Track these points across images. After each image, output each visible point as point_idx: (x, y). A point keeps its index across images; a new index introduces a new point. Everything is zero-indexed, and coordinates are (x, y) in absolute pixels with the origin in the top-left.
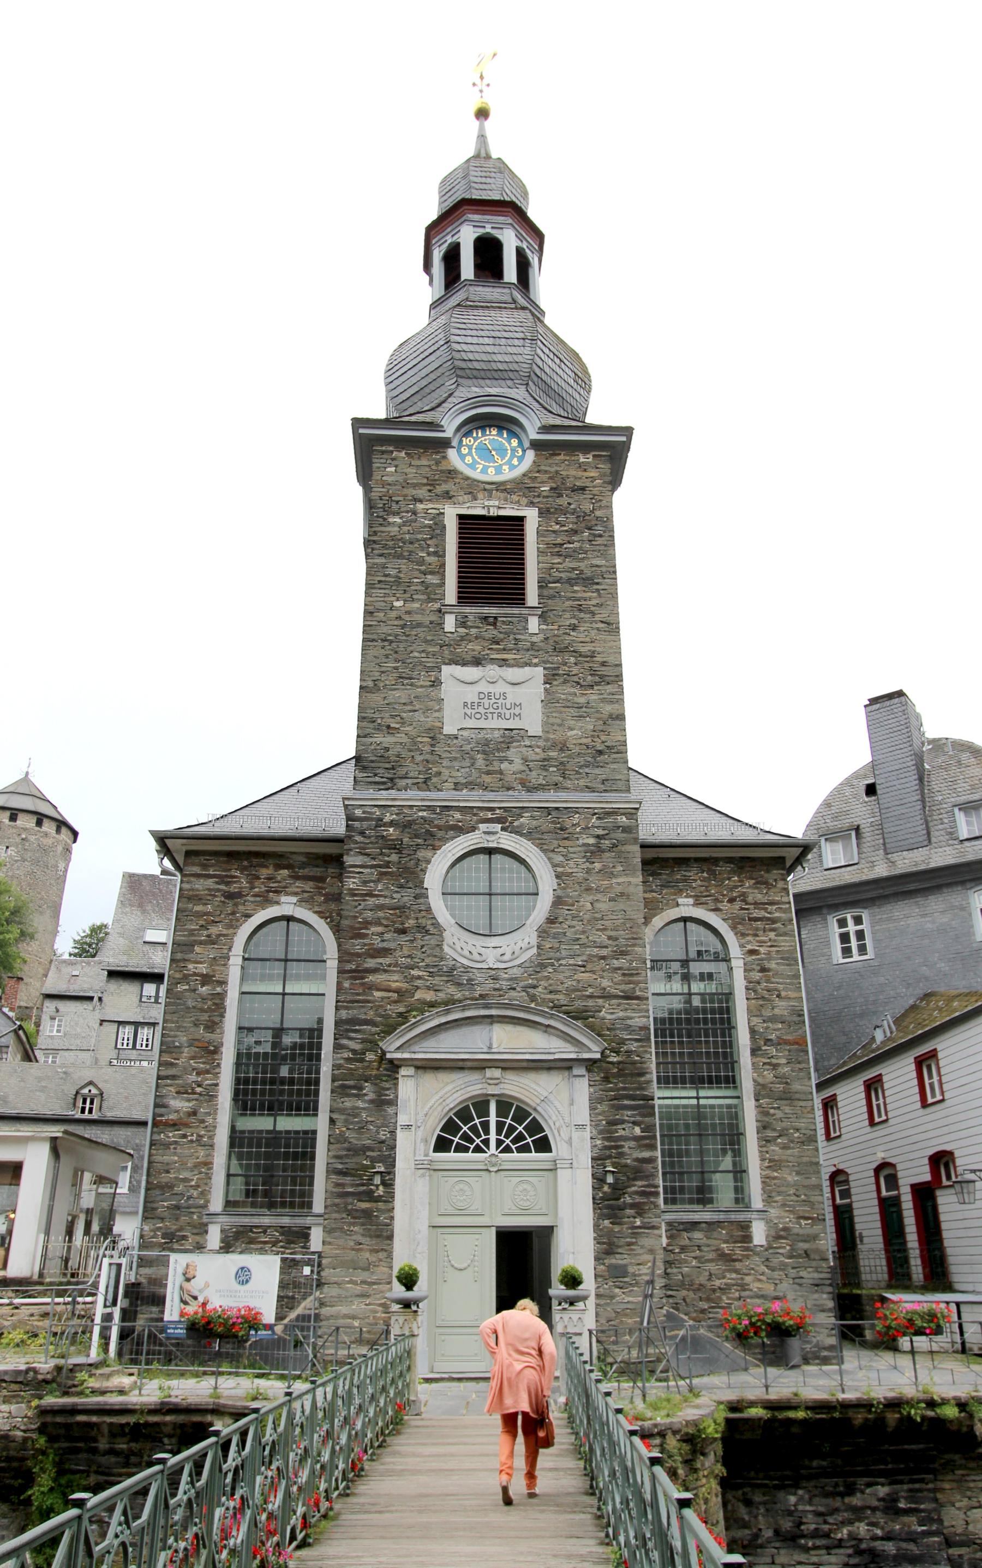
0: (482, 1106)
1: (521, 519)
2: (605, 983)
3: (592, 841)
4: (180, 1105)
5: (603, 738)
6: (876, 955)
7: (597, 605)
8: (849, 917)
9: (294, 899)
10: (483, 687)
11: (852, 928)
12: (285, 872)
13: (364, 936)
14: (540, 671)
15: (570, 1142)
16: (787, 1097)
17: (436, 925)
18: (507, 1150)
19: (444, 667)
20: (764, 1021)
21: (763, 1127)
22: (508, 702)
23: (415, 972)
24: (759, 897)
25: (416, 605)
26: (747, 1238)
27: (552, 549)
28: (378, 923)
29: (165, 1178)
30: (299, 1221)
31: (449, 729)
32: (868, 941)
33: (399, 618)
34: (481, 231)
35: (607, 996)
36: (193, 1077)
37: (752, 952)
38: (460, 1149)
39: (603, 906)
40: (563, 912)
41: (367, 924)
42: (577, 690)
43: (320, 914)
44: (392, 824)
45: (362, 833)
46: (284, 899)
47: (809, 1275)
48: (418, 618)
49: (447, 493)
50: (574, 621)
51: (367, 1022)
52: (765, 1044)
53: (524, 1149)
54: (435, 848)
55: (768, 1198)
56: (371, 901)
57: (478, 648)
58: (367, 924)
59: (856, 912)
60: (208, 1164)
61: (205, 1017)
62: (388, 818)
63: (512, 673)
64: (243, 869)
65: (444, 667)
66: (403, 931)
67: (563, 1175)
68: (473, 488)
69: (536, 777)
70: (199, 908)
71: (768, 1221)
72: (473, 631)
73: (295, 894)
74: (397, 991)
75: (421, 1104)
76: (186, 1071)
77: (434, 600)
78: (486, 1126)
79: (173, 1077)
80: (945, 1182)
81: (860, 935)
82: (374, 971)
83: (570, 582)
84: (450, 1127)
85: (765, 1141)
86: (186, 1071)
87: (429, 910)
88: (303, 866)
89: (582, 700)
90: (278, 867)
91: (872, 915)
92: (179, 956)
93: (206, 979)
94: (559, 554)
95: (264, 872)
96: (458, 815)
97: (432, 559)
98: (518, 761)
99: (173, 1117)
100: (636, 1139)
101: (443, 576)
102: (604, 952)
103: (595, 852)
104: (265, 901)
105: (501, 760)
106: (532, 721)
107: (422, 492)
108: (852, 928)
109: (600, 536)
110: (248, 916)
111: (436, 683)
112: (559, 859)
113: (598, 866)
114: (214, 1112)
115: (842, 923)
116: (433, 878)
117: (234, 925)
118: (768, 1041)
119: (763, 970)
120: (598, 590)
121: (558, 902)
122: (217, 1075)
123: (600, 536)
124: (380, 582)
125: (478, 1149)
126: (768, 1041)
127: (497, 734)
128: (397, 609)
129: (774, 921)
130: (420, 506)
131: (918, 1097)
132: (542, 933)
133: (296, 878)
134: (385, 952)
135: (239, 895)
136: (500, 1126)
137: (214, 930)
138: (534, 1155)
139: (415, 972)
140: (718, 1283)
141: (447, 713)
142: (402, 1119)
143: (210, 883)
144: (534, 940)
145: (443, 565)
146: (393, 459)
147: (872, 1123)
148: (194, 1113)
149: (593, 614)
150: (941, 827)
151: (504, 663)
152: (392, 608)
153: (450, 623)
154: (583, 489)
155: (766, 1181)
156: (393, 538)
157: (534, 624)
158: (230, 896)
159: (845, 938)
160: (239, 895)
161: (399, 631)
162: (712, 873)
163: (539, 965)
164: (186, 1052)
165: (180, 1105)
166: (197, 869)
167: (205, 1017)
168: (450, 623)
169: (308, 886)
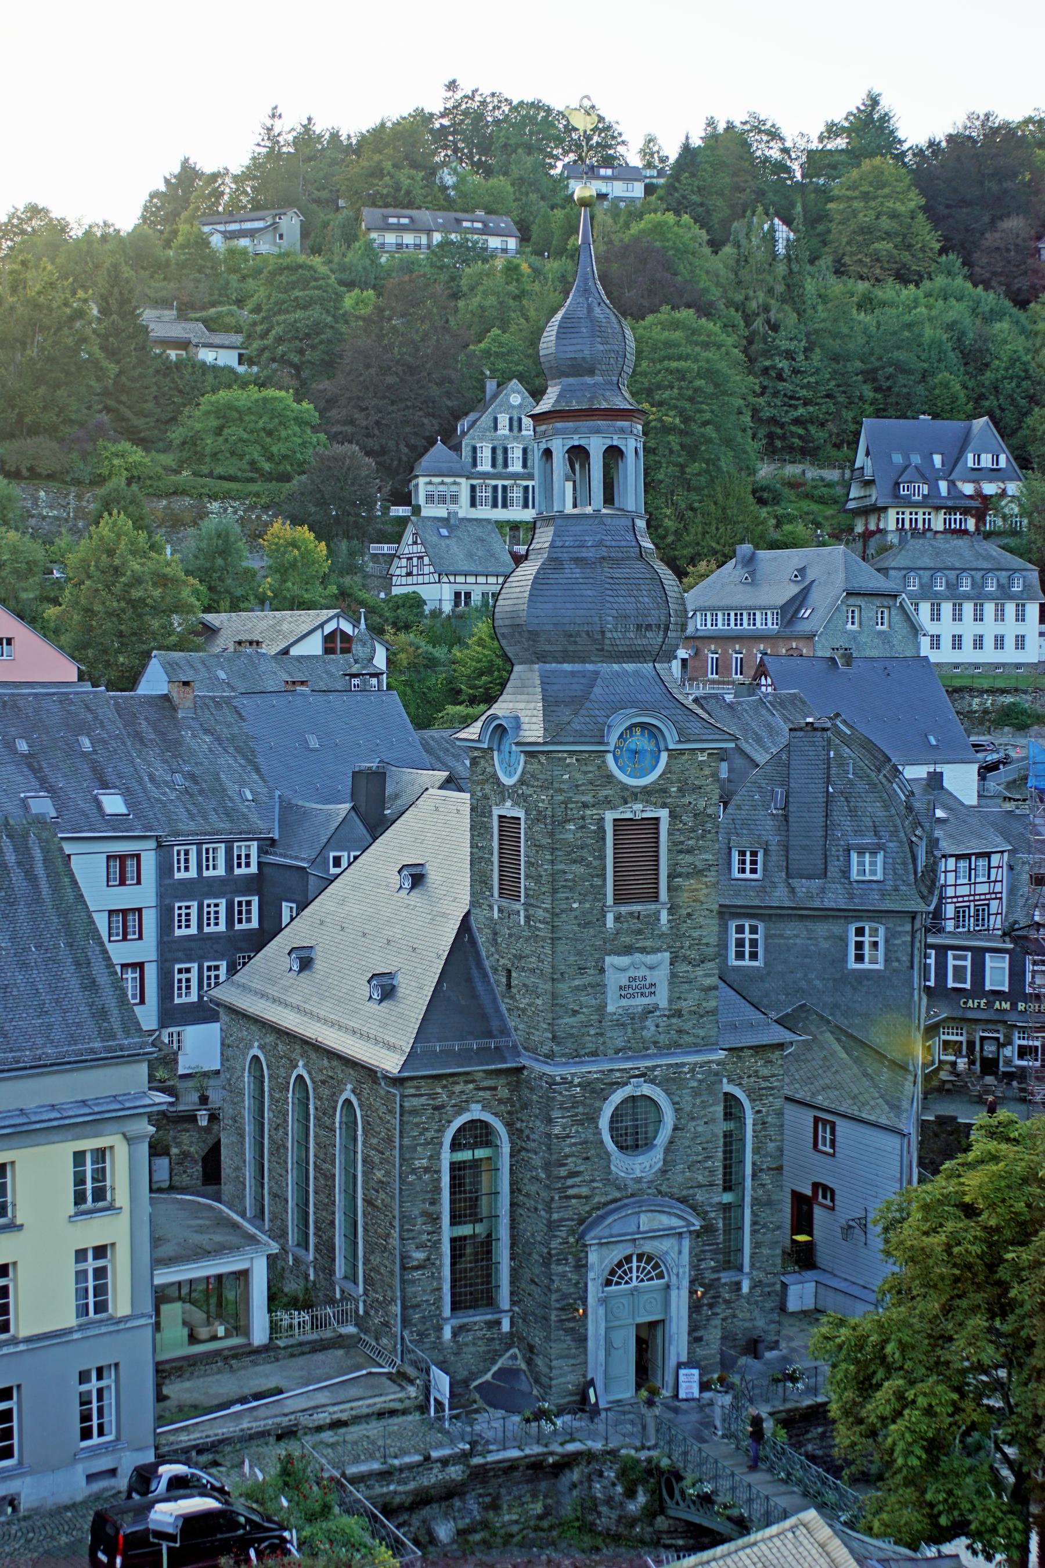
0: (628, 1259)
1: (657, 819)
2: (700, 1178)
3: (695, 1084)
4: (420, 1255)
5: (705, 1004)
6: (765, 963)
9: (479, 1106)
10: (632, 973)
11: (747, 935)
12: (471, 1086)
13: (565, 1165)
14: (667, 955)
15: (678, 1275)
16: (769, 1203)
18: (642, 1281)
19: (607, 958)
21: (754, 1223)
22: (647, 983)
23: (595, 1185)
24: (765, 1072)
25: (587, 906)
26: (739, 1289)
27: (677, 849)
28: (573, 1155)
29: (414, 1301)
30: (496, 1316)
31: (610, 1009)
32: (760, 951)
34: (609, 442)
35: (700, 1186)
36: (425, 1237)
37: (759, 1112)
38: (618, 1283)
39: (700, 1129)
40: (679, 1133)
41: (567, 1157)
42: (689, 968)
43: (495, 1114)
44: (579, 1085)
45: (560, 1093)
46: (473, 1106)
47: (769, 1305)
48: (589, 918)
49: (606, 797)
50: (689, 910)
51: (568, 1219)
53: (651, 1279)
54: (606, 1099)
55: (752, 1265)
56: (568, 1141)
57: (628, 939)
58: (567, 1157)
59: (754, 922)
60: (439, 1289)
61: (429, 1196)
62: (577, 1081)
63: (650, 959)
64: (444, 1087)
65: (607, 958)
66: (587, 1158)
67: (674, 1293)
68: (628, 795)
69: (663, 1039)
70: (416, 1120)
71: (752, 1279)
72: (625, 926)
73: (478, 1102)
74: (586, 1197)
75: (599, 1261)
76: (420, 1233)
77: (599, 900)
78: (631, 1269)
79: (413, 1238)
81: (754, 943)
82: (572, 1187)
83: (688, 876)
84: (613, 1273)
85: (754, 1232)
86: (420, 1233)
87: (602, 1142)
88: (483, 1079)
90: (467, 1082)
91: (766, 929)
93: (427, 1170)
94: (681, 852)
95: (458, 1088)
96: (618, 1074)
97: (596, 863)
98: (653, 1028)
99: (415, 1263)
100: (712, 1268)
101: (605, 880)
102: (700, 1158)
103: (696, 1093)
104: (460, 1110)
106: (662, 999)
107: (588, 798)
108: (747, 935)
109: (710, 832)
110: (450, 1122)
111: (602, 971)
113: (698, 1101)
114: (440, 1256)
115: (740, 929)
116: (604, 1123)
117: (441, 1131)
118: (761, 1170)
119: (764, 1123)
120: (705, 883)
121: (676, 1128)
122: (439, 1234)
123: (710, 832)
124: (564, 887)
125: (627, 1283)
126: (761, 1170)
127: (640, 1009)
129: (772, 1088)
130: (588, 812)
132: (667, 1151)
133: (478, 1089)
134: (577, 1174)
135: (443, 1107)
136: (638, 1267)
137: (429, 1135)
138: (656, 1282)
139: (595, 1185)
141: (609, 995)
142: (591, 1275)
143: (423, 1100)
144: (661, 1156)
145: (604, 868)
146: (568, 765)
148: (428, 1259)
151: (643, 950)
152: (572, 910)
155: (753, 1255)
157: (664, 916)
158: (436, 1108)
159: (740, 943)
160: (443, 1107)
161: (576, 928)
162: (739, 1057)
163: (664, 1172)
164: (419, 1221)
166: (412, 1091)
167: (429, 1196)
169: (487, 1094)
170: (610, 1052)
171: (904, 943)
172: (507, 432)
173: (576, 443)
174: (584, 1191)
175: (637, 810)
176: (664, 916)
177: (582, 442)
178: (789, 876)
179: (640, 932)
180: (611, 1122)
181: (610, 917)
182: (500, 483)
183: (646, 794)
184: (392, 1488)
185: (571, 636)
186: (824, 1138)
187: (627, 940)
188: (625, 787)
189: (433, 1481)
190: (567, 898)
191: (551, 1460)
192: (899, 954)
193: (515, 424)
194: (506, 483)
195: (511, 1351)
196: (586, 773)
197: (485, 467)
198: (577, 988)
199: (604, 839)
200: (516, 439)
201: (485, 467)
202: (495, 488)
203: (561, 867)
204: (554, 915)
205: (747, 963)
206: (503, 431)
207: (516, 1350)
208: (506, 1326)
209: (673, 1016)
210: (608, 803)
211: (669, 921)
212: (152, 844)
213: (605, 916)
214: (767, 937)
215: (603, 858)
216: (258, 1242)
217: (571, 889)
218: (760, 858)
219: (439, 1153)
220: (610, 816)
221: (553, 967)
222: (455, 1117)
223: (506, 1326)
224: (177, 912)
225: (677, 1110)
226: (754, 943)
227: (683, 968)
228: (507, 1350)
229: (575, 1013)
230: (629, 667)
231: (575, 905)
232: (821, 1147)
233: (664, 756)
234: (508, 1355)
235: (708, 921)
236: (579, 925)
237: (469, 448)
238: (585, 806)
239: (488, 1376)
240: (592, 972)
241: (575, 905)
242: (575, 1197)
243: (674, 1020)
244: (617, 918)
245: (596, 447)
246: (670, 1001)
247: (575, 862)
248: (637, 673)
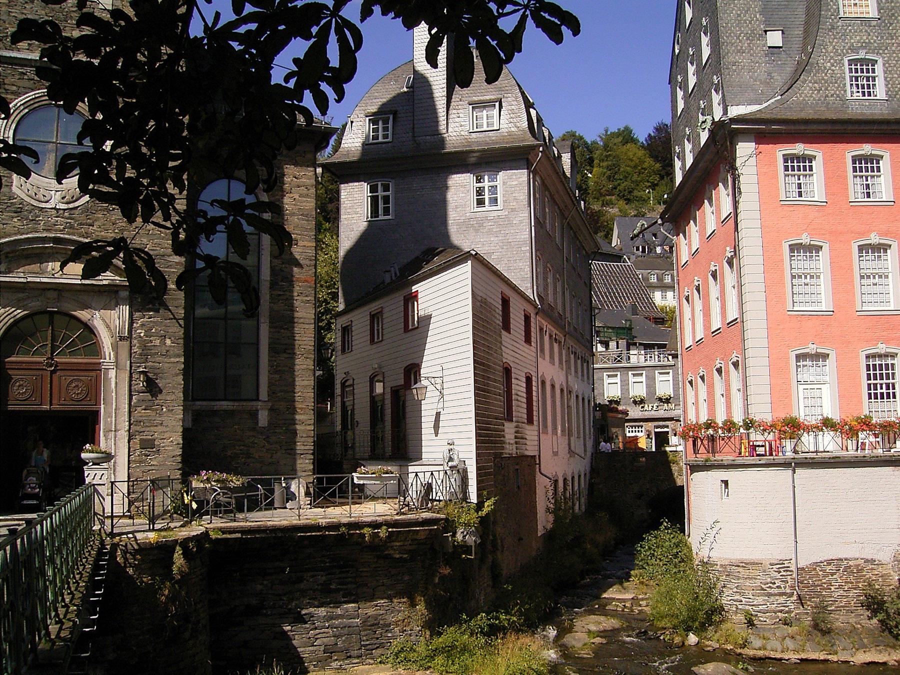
8: (379, 183)
11: (380, 193)
20: (283, 263)
52: (282, 281)
81: (386, 200)
131: (402, 325)
140: (229, 453)
147: (372, 341)
150: (457, 120)
205: (381, 218)
214: (396, 193)
226: (386, 200)
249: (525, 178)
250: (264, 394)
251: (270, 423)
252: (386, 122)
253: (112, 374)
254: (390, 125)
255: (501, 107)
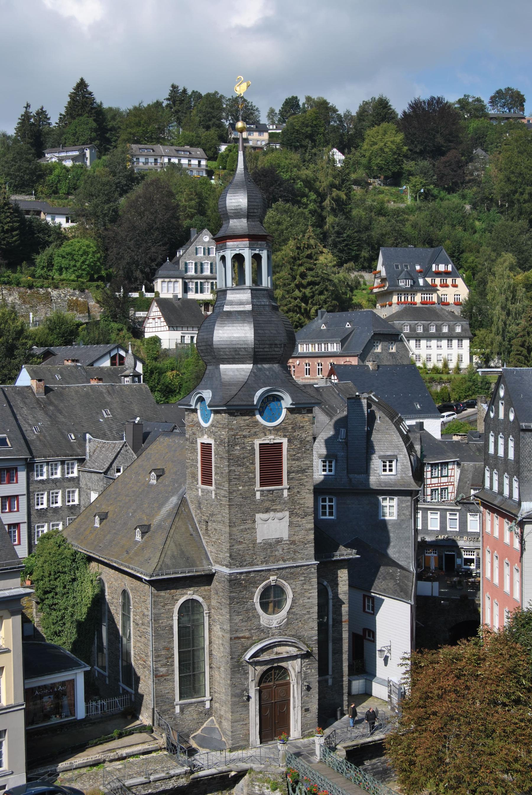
1: (281, 443)
4: (163, 670)
6: (337, 517)
7: (307, 482)
11: (327, 504)
17: (258, 615)
25: (246, 488)
27: (292, 458)
31: (258, 541)
33: (241, 494)
42: (299, 519)
49: (255, 432)
55: (333, 671)
63: (279, 515)
68: (265, 431)
72: (266, 498)
80: (367, 637)
81: (331, 507)
83: (298, 472)
89: (301, 523)
92: (156, 618)
105: (275, 551)
108: (327, 504)
109: (308, 450)
110: (178, 600)
111: (254, 521)
112: (293, 586)
115: (324, 500)
120: (306, 476)
123: (308, 450)
128: (240, 490)
137: (167, 607)
149: (305, 486)
151: (275, 510)
153: (258, 495)
154: (303, 427)
156: (238, 457)
157: (286, 493)
161: (241, 499)
163: (287, 624)
165: (163, 670)
168: (258, 495)
170: (260, 562)
171: (407, 506)
172: (202, 255)
173: (238, 252)
174: (247, 634)
175: (270, 439)
176: (286, 493)
177: (241, 252)
178: (348, 473)
179: (273, 501)
180: (261, 599)
181: (258, 495)
182: (199, 281)
183: (276, 430)
184: (150, 791)
185: (236, 351)
186: (369, 606)
187: (267, 504)
188: (265, 427)
189: (171, 787)
190: (236, 484)
191: (233, 773)
192: (404, 512)
193: (207, 251)
194: (202, 281)
195: (211, 718)
196: (245, 420)
197: (192, 272)
198: (242, 531)
199: (254, 454)
200: (207, 259)
201: (192, 272)
202: (197, 283)
203: (233, 468)
204: (230, 493)
205: (328, 517)
206: (201, 254)
207: (213, 718)
208: (208, 705)
209: (291, 544)
210: (255, 434)
211: (288, 495)
212: (24, 463)
213: (255, 493)
214: (337, 504)
215: (253, 463)
216: (80, 665)
217: (238, 479)
218: (333, 464)
219: (172, 617)
220: (257, 442)
221: (229, 519)
222: (180, 598)
223: (208, 705)
224: (36, 497)
225: (293, 592)
226: (331, 507)
227: (295, 519)
228: (208, 718)
229: (241, 543)
230: (266, 366)
231: (240, 488)
232: (367, 610)
233: (284, 411)
234: (209, 720)
235: (308, 496)
236: (243, 498)
237: (183, 264)
238: (245, 437)
239: (199, 732)
240: (249, 521)
241: (240, 488)
242: (243, 637)
243: (292, 546)
244: (262, 495)
245: (247, 254)
246: (290, 536)
247: (240, 466)
248: (269, 369)
249: (409, 504)
250: (330, 672)
251: (333, 683)
252: (330, 462)
253: (295, 686)
254: (333, 464)
255: (397, 460)
